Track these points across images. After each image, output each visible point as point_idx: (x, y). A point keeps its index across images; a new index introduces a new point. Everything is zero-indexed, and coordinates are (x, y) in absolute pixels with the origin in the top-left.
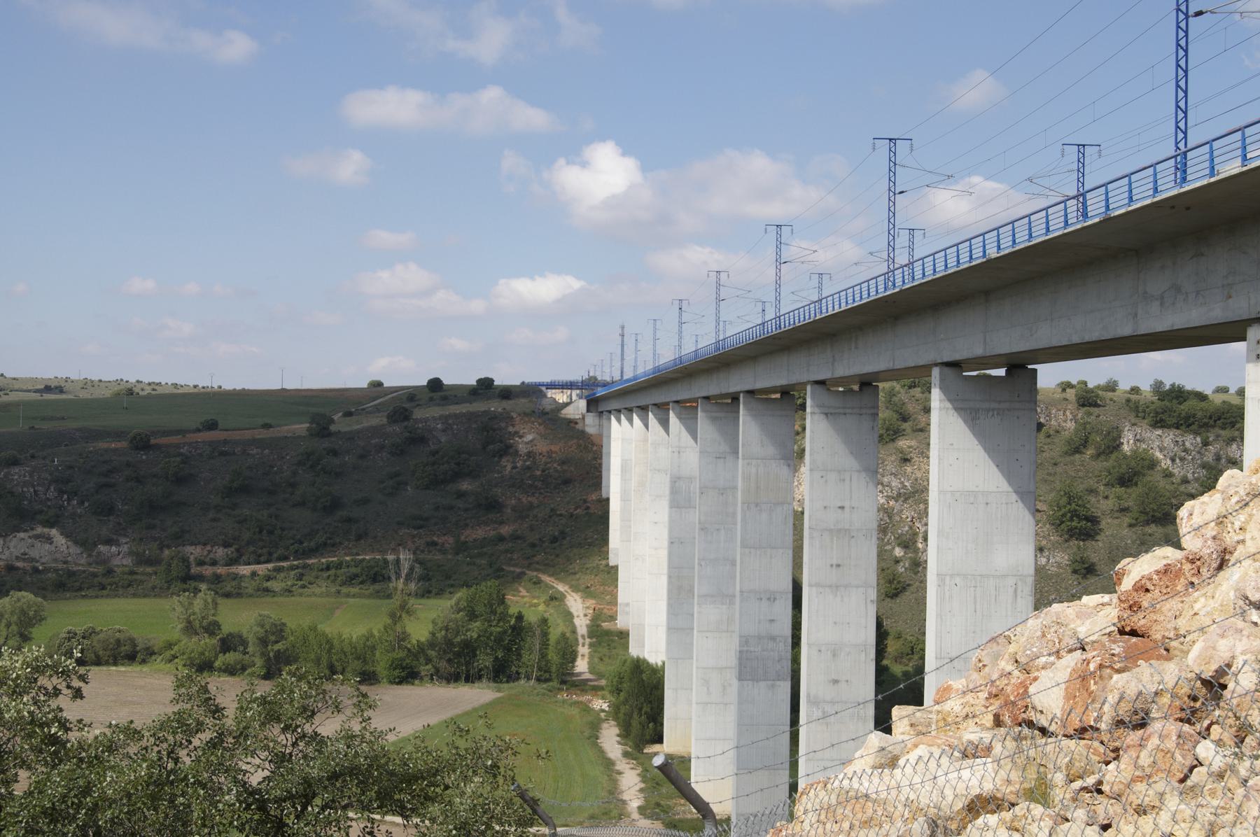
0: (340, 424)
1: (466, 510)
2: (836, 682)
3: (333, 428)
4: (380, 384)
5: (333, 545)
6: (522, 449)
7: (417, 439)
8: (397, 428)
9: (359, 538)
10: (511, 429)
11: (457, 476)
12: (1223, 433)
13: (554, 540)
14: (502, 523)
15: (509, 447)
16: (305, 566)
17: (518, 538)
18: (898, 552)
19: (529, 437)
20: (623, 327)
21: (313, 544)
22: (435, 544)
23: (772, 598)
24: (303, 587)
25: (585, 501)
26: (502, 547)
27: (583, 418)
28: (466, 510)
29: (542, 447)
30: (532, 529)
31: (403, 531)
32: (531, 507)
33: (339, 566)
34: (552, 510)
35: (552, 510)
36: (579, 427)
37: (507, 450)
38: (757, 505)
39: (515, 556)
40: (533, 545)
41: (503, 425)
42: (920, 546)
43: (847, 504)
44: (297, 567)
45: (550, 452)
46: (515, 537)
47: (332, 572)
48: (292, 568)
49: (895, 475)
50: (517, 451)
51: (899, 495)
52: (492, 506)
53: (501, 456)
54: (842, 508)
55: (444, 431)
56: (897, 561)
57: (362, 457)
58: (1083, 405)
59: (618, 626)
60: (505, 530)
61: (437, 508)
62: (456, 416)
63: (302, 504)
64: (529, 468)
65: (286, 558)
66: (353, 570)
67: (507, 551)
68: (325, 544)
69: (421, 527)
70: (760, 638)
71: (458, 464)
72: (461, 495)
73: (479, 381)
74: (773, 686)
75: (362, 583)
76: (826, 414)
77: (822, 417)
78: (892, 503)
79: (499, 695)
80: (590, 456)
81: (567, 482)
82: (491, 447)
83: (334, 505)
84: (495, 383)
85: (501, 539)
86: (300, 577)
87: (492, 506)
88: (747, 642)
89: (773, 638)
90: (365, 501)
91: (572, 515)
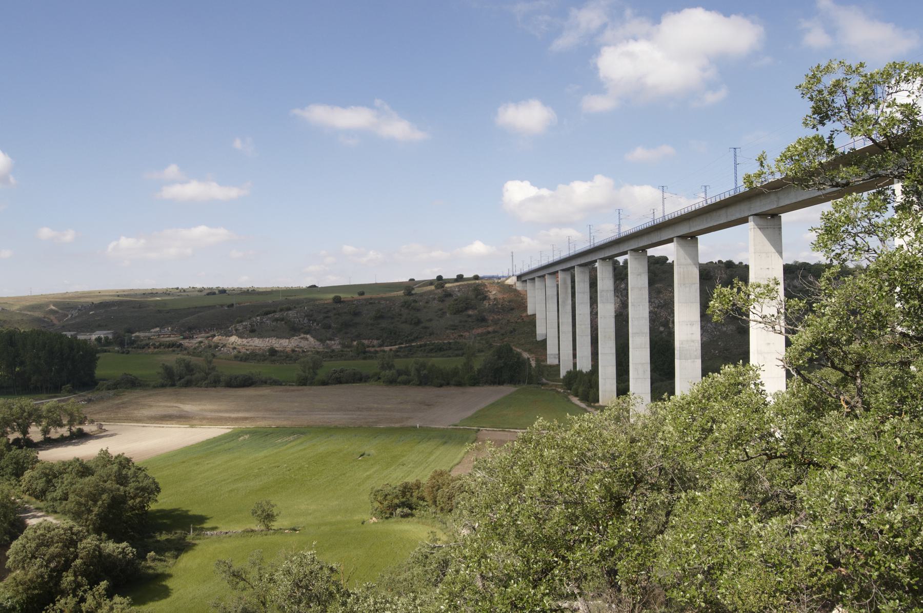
0: (417, 290)
1: (473, 322)
2: (769, 344)
3: (413, 292)
4: (413, 280)
5: (421, 338)
6: (492, 297)
7: (448, 295)
8: (439, 291)
9: (430, 334)
10: (486, 289)
11: (467, 309)
12: (790, 276)
13: (511, 332)
14: (488, 326)
15: (486, 296)
16: (412, 346)
17: (496, 332)
18: (662, 329)
19: (494, 292)
20: (512, 253)
21: (412, 338)
22: (462, 336)
23: (692, 324)
24: (412, 354)
25: (521, 316)
26: (490, 336)
27: (515, 284)
28: (473, 322)
29: (500, 296)
30: (501, 328)
31: (448, 331)
32: (499, 320)
33: (425, 345)
34: (508, 321)
35: (508, 321)
36: (514, 287)
37: (485, 298)
38: (684, 285)
39: (496, 339)
40: (503, 335)
41: (483, 288)
42: (670, 326)
43: (770, 267)
44: (408, 346)
45: (503, 298)
46: (495, 332)
47: (423, 348)
48: (406, 347)
49: (656, 298)
50: (489, 298)
51: (659, 306)
52: (482, 320)
53: (484, 300)
54: (768, 269)
55: (459, 291)
56: (661, 332)
57: (427, 303)
58: (728, 268)
59: (548, 363)
60: (490, 329)
61: (460, 322)
62: (462, 285)
63: (406, 322)
64: (495, 304)
65: (402, 344)
66: (432, 347)
67: (492, 337)
68: (417, 338)
69: (455, 329)
70: (687, 341)
71: (467, 304)
72: (469, 316)
73: (457, 276)
74: (694, 361)
75: (436, 351)
76: (760, 229)
77: (758, 229)
78: (656, 309)
79: (517, 389)
80: (520, 299)
81: (512, 309)
82: (479, 297)
83: (418, 322)
84: (464, 277)
85: (489, 333)
86: (410, 350)
87: (482, 320)
88: (682, 343)
89: (693, 341)
90: (430, 320)
91: (516, 322)
